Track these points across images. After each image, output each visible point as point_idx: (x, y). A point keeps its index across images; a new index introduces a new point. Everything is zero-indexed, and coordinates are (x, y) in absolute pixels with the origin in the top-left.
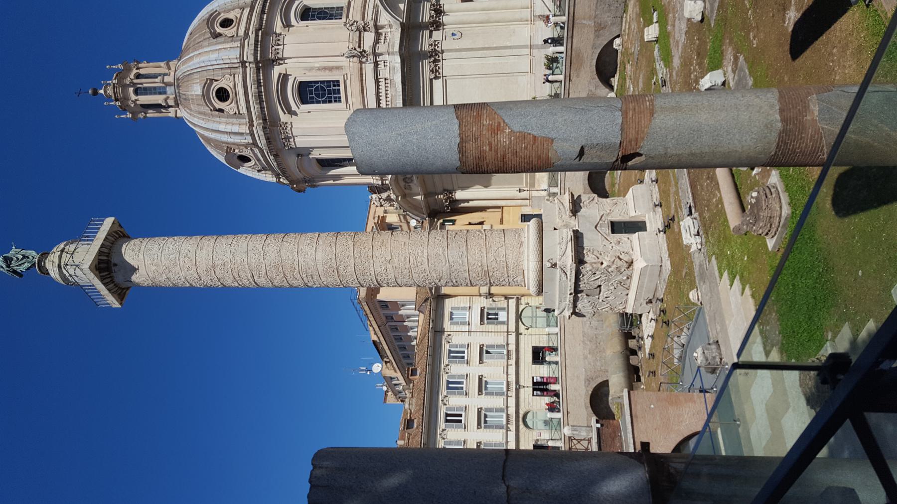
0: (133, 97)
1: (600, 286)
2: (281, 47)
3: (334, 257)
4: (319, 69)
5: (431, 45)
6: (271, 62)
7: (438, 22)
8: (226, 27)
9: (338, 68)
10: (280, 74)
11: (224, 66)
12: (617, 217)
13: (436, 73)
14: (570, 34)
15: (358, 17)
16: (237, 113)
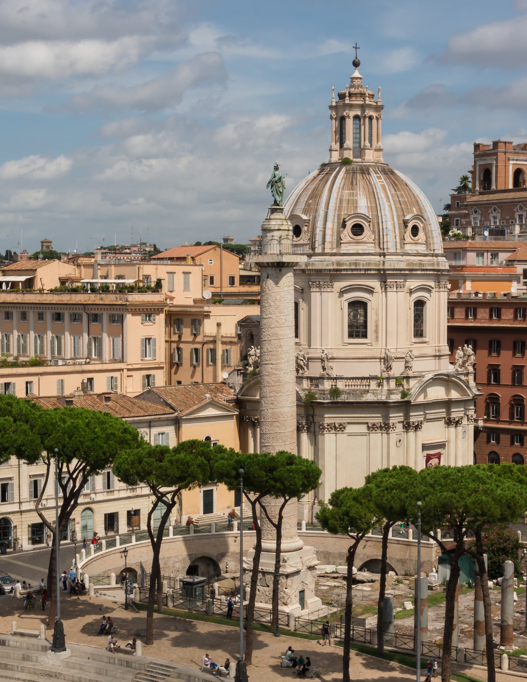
0: (352, 114)
1: (268, 586)
2: (395, 290)
3: (286, 419)
4: (377, 322)
5: (393, 424)
6: (384, 280)
7: (409, 428)
8: (412, 233)
9: (377, 337)
10: (374, 288)
11: (381, 234)
12: (307, 593)
13: (372, 428)
14: (401, 542)
15: (415, 353)
16: (342, 242)
